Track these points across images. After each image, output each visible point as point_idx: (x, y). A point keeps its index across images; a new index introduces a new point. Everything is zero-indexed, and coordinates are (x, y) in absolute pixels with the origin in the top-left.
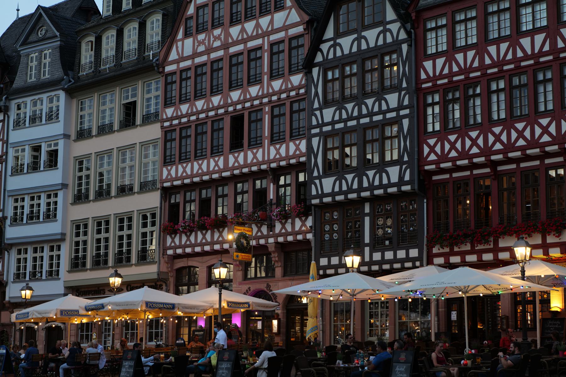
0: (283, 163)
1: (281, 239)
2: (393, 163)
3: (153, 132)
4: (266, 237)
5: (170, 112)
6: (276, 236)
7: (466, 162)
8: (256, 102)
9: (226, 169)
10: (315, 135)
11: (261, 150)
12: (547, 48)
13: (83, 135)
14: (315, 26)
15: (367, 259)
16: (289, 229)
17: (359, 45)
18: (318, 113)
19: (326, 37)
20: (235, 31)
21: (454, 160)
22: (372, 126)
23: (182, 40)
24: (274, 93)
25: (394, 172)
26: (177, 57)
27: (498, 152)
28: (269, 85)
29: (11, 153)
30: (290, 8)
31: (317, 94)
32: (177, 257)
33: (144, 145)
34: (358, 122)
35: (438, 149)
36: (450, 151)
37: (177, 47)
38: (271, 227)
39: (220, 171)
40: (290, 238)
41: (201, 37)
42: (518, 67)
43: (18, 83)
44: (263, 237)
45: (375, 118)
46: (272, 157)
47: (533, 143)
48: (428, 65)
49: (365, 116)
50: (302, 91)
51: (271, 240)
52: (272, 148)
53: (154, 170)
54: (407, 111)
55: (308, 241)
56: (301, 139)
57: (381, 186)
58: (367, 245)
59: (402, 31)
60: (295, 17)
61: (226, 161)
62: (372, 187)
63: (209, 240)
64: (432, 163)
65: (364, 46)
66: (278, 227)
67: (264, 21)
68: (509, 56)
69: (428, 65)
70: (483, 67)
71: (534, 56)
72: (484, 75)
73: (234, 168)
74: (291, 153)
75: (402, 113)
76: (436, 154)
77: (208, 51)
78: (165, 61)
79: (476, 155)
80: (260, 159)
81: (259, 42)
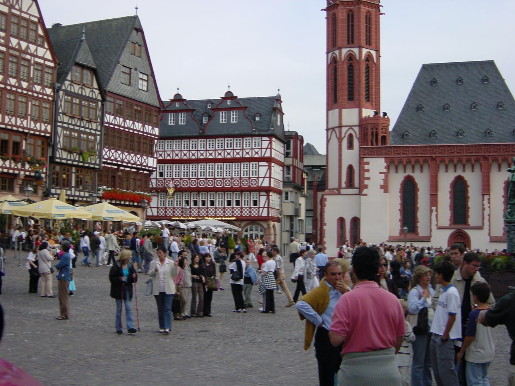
1: (28, 173)
6: (25, 171)
10: (60, 126)
17: (82, 92)
20: (14, 42)
21: (112, 160)
31: (61, 105)
38: (23, 165)
44: (18, 169)
46: (32, 127)
50: (50, 99)
51: (22, 173)
52: (32, 122)
58: (73, 187)
59: (99, 95)
67: (32, 47)
69: (108, 116)
75: (98, 133)
81: (28, 57)
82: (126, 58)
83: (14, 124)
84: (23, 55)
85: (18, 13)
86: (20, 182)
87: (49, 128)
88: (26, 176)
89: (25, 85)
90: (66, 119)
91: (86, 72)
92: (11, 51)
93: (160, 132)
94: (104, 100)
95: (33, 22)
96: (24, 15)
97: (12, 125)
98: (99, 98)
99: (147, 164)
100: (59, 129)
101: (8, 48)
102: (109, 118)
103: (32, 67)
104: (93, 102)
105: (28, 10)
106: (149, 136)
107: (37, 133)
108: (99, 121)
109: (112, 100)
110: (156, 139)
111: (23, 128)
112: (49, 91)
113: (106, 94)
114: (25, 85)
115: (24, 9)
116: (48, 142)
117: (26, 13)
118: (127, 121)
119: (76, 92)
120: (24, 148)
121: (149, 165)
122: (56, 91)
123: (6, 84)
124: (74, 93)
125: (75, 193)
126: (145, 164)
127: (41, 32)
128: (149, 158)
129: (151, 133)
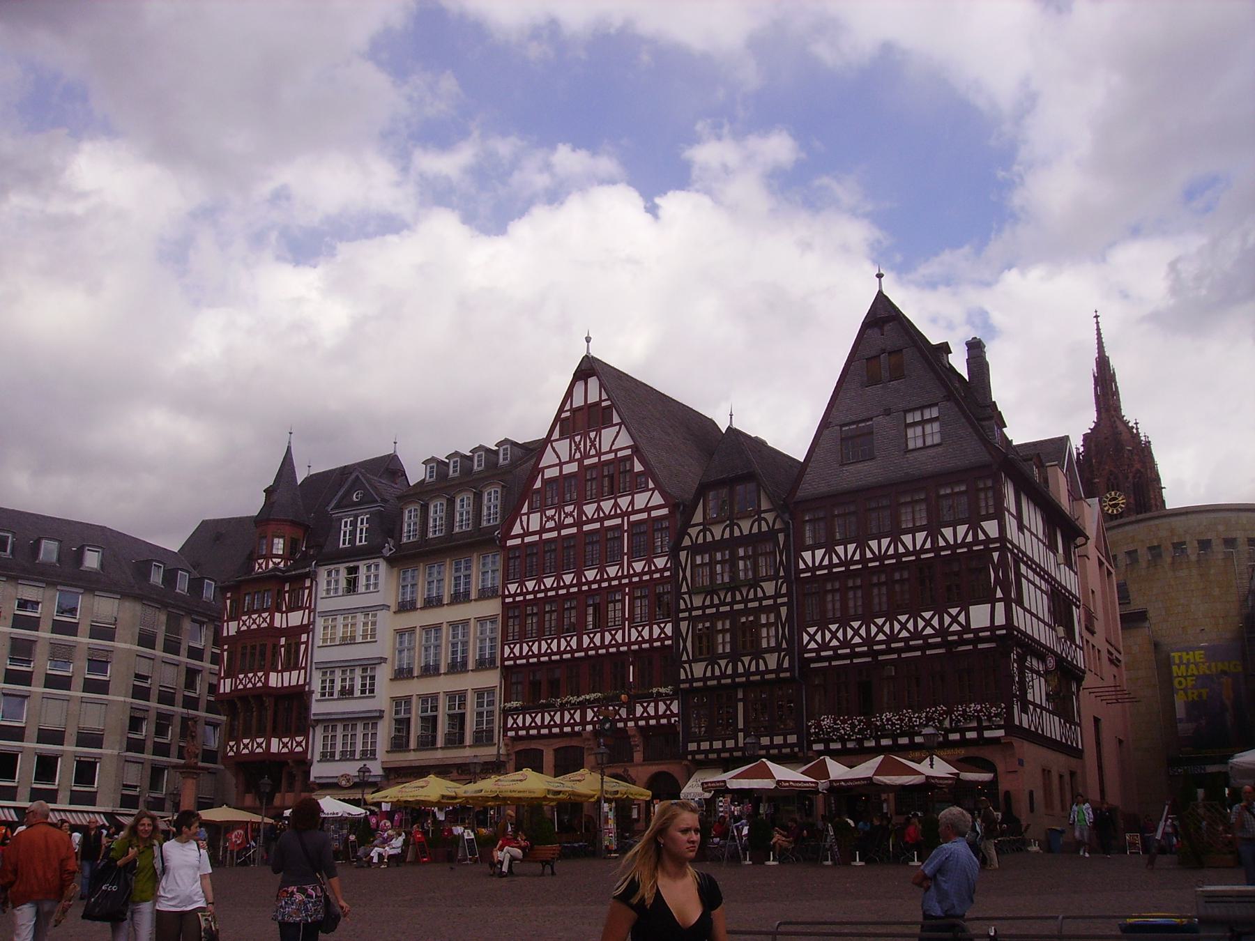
0: (645, 646)
1: (642, 723)
2: (770, 650)
3: (492, 607)
4: (625, 721)
5: (513, 588)
6: (636, 720)
8: (615, 583)
10: (684, 619)
11: (620, 632)
12: (928, 545)
13: (405, 607)
14: (681, 510)
15: (741, 744)
16: (652, 713)
17: (732, 532)
21: (835, 649)
22: (746, 612)
23: (528, 514)
24: (636, 574)
25: (772, 661)
27: (880, 642)
28: (629, 565)
29: (320, 622)
30: (654, 490)
31: (685, 577)
32: (518, 738)
33: (481, 620)
34: (732, 608)
35: (818, 637)
36: (830, 640)
39: (572, 651)
40: (653, 722)
41: (550, 513)
42: (899, 562)
44: (621, 720)
45: (750, 605)
46: (633, 639)
47: (916, 634)
48: (807, 555)
50: (667, 574)
51: (631, 724)
53: (492, 648)
54: (785, 600)
56: (666, 623)
57: (758, 672)
58: (741, 730)
60: (657, 499)
61: (580, 642)
62: (747, 673)
64: (811, 651)
65: (737, 533)
66: (639, 710)
67: (624, 502)
68: (891, 551)
69: (807, 555)
70: (863, 560)
71: (915, 552)
72: (865, 567)
73: (588, 649)
74: (655, 636)
75: (779, 601)
76: (816, 642)
77: (560, 526)
78: (507, 535)
79: (859, 645)
81: (618, 521)
85: (596, 460)
87: (669, 629)
90: (697, 601)
92: (586, 528)
96: (604, 458)
99: (967, 628)
100: (684, 626)
108: (782, 574)
110: (995, 549)
111: (618, 645)
117: (610, 451)
126: (955, 627)
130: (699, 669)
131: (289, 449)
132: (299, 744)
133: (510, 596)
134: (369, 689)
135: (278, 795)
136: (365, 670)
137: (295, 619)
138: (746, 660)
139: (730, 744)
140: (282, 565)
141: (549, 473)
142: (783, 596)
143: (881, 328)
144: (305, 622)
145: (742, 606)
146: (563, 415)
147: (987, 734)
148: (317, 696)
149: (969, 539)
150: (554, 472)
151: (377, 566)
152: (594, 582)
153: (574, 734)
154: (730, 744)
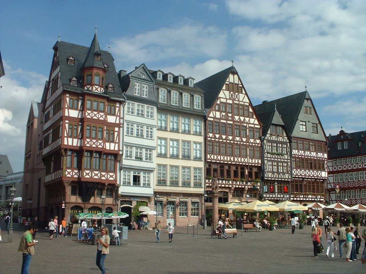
4: (245, 186)
5: (211, 135)
6: (248, 186)
7: (301, 177)
9: (234, 161)
10: (266, 160)
11: (246, 159)
12: (316, 156)
15: (276, 196)
17: (277, 139)
18: (266, 153)
19: (268, 133)
20: (237, 118)
21: (299, 176)
22: (281, 162)
26: (213, 116)
27: (307, 176)
29: (125, 124)
31: (266, 148)
37: (213, 113)
38: (246, 183)
41: (224, 114)
43: (128, 93)
45: (282, 160)
46: (250, 162)
49: (279, 159)
50: (259, 145)
52: (250, 159)
54: (289, 161)
55: (258, 189)
60: (256, 122)
61: (234, 159)
62: (281, 178)
63: (224, 183)
66: (249, 184)
67: (247, 119)
69: (294, 151)
71: (314, 157)
75: (288, 161)
80: (246, 162)
81: (245, 125)
82: (302, 116)
83: (240, 161)
84: (242, 124)
85: (238, 102)
86: (246, 192)
87: (260, 161)
88: (249, 188)
89: (244, 140)
90: (269, 156)
91: (278, 127)
92: (236, 123)
93: (328, 156)
94: (290, 142)
95: (246, 106)
96: (240, 103)
97: (239, 162)
98: (288, 141)
99: (321, 177)
100: (266, 161)
101: (234, 121)
102: (295, 152)
103: (248, 130)
104: (284, 144)
105: (243, 100)
106: (321, 159)
107: (253, 165)
108: (289, 154)
109: (296, 141)
111: (245, 163)
112: (258, 141)
113: (291, 138)
114: (244, 140)
115: (241, 100)
116: (261, 169)
117: (242, 102)
118: (306, 152)
119: (274, 139)
120: (247, 174)
121: (322, 176)
122: (262, 141)
123: (234, 141)
124: (273, 140)
125: (277, 196)
126: (320, 176)
127: (251, 110)
128: (322, 172)
129: (322, 157)
130: (270, 175)
131: (95, 35)
132: (111, 176)
133: (209, 137)
134: (149, 159)
135: (92, 198)
136: (147, 151)
137: (111, 119)
138: (281, 174)
139: (274, 196)
140: (103, 92)
141: (222, 100)
142: (289, 160)
143: (308, 100)
144: (118, 122)
145: (280, 160)
146: (226, 83)
147: (321, 200)
148: (124, 157)
149: (322, 157)
150: (224, 100)
151: (152, 109)
152: (239, 141)
153: (229, 188)
154: (274, 196)
